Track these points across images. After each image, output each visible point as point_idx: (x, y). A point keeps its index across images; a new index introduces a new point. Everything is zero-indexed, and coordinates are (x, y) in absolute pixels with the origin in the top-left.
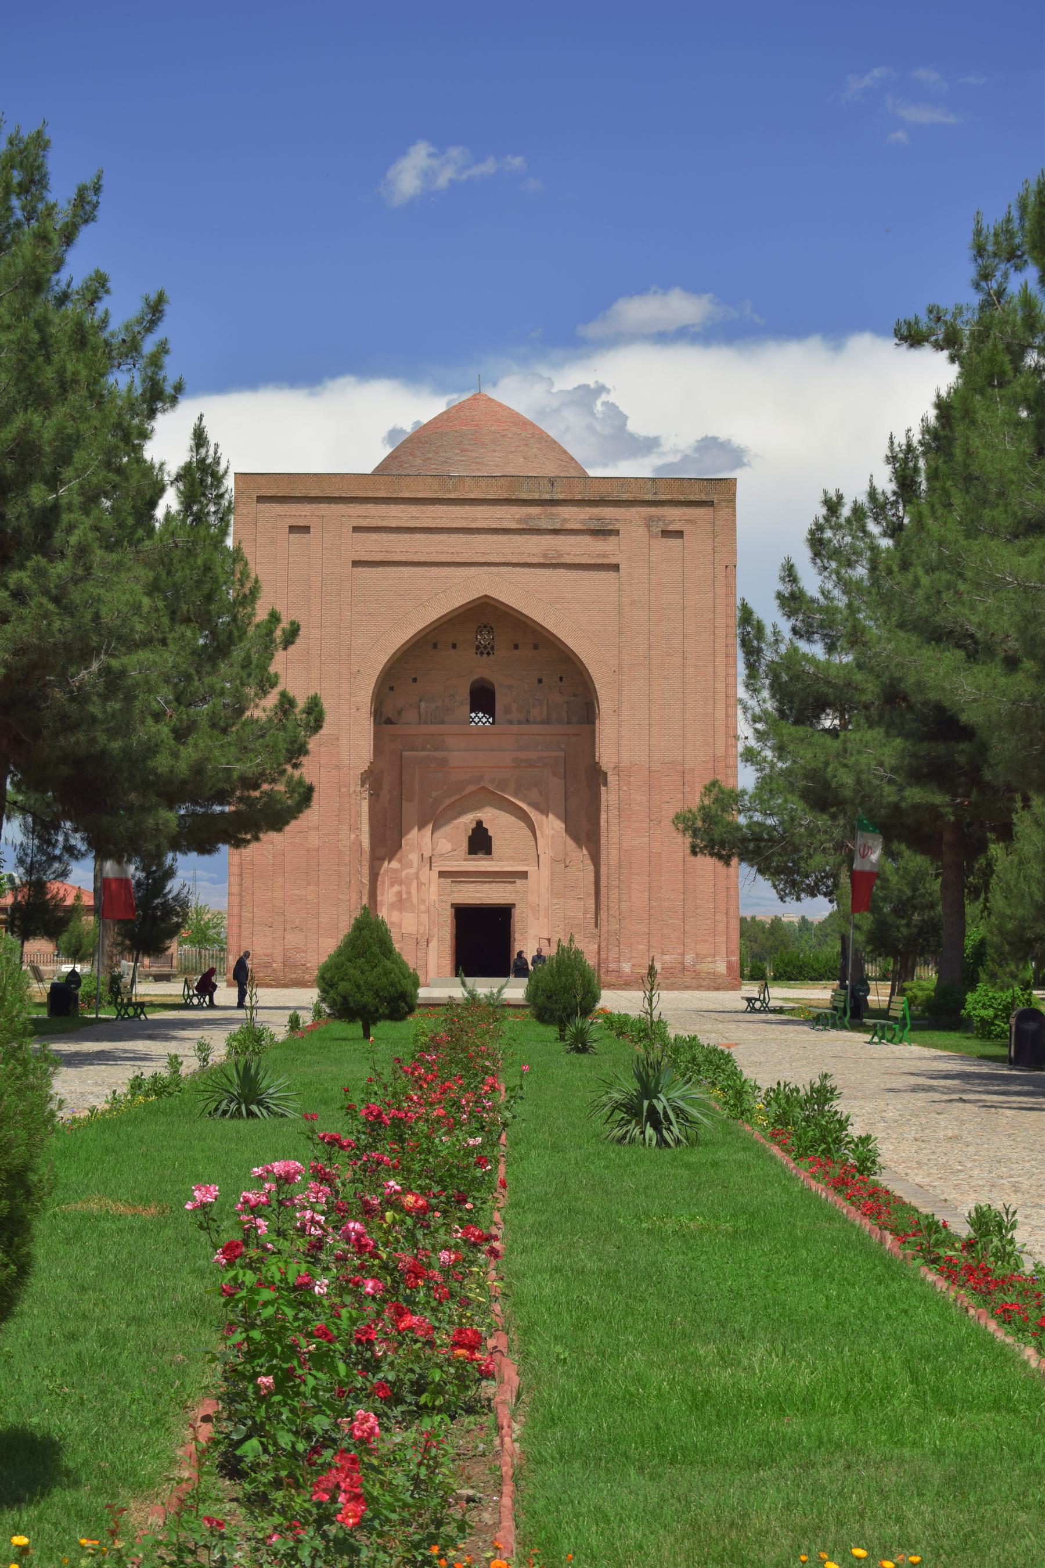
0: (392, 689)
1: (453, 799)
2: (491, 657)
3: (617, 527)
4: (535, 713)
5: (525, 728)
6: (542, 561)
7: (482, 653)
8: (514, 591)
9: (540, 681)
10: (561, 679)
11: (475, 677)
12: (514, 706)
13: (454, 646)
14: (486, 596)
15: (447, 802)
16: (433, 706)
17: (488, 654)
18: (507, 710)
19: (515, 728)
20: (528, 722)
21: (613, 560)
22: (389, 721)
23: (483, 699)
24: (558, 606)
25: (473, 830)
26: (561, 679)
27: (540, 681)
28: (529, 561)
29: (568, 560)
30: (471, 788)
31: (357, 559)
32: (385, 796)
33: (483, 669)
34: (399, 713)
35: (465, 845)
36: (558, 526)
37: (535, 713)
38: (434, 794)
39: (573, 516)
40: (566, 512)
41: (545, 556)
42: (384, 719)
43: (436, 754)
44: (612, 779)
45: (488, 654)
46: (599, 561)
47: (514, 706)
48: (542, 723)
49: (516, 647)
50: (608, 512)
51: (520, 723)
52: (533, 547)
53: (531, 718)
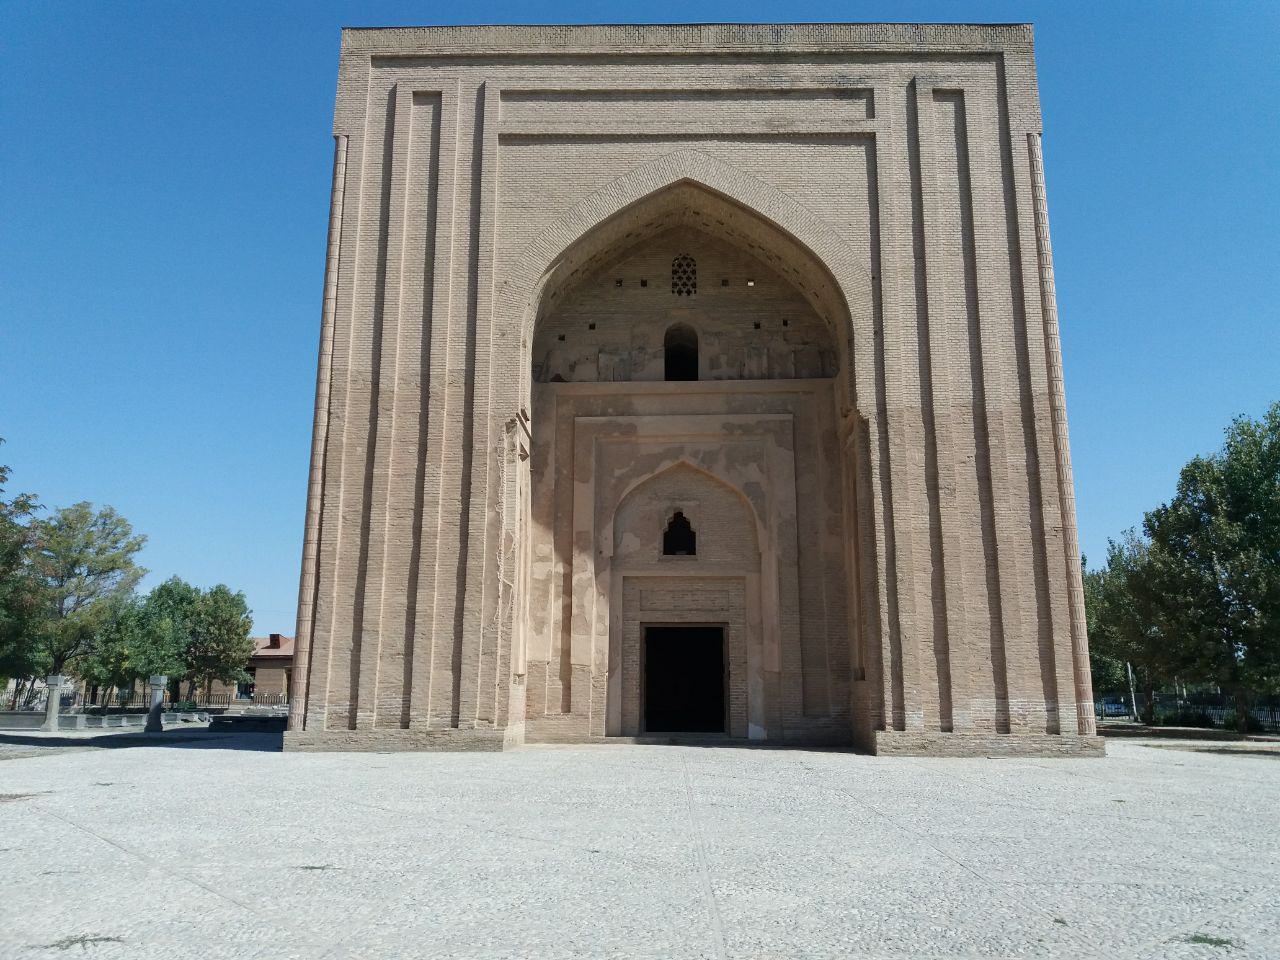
0: (562, 338)
1: (645, 478)
2: (693, 296)
3: (869, 86)
4: (752, 366)
5: (740, 385)
6: (765, 130)
7: (680, 292)
8: (724, 171)
9: (757, 326)
10: (785, 323)
11: (670, 324)
12: (723, 359)
13: (644, 284)
14: (687, 183)
15: (635, 483)
16: (617, 359)
17: (689, 293)
18: (714, 364)
19: (725, 385)
20: (741, 377)
21: (867, 126)
22: (558, 379)
23: (681, 362)
24: (788, 191)
25: (670, 525)
26: (785, 323)
27: (757, 326)
28: (746, 131)
29: (803, 129)
30: (666, 465)
31: (506, 131)
32: (550, 473)
33: (682, 312)
34: (572, 368)
35: (658, 543)
36: (786, 86)
37: (752, 366)
38: (617, 473)
39: (805, 75)
40: (795, 69)
41: (769, 123)
42: (551, 376)
43: (621, 419)
44: (874, 428)
45: (689, 293)
46: (847, 129)
47: (723, 359)
48: (762, 377)
49: (725, 283)
50: (856, 70)
51: (730, 378)
52: (753, 115)
53: (746, 373)
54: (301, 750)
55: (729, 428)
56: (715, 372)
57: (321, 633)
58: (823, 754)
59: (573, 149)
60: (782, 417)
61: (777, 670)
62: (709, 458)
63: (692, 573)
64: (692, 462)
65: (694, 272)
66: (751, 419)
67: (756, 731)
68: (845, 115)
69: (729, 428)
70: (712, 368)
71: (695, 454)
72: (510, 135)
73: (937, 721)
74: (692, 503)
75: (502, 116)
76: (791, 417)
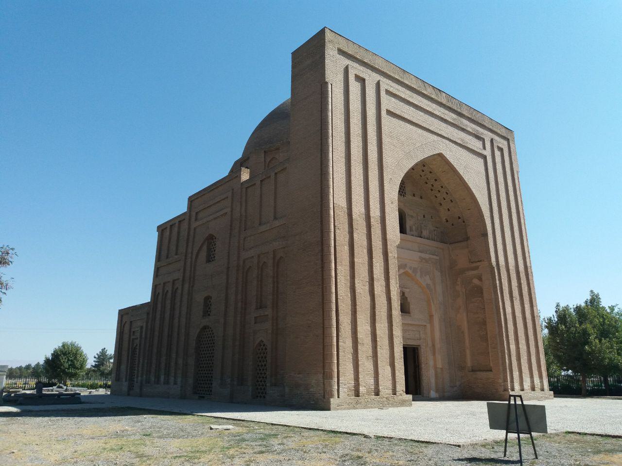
4: (425, 233)
12: (414, 227)
14: (440, 155)
20: (420, 237)
45: (404, 196)
49: (414, 195)
53: (422, 236)
54: (338, 409)
55: (421, 259)
56: (412, 233)
57: (342, 344)
58: (263, 412)
59: (420, 131)
60: (435, 257)
61: (441, 367)
62: (415, 270)
63: (410, 322)
64: (410, 272)
65: (405, 187)
66: (427, 256)
67: (433, 394)
68: (476, 145)
69: (421, 259)
70: (410, 231)
71: (410, 268)
72: (391, 112)
73: (390, 391)
74: (408, 290)
75: (388, 103)
76: (438, 258)
